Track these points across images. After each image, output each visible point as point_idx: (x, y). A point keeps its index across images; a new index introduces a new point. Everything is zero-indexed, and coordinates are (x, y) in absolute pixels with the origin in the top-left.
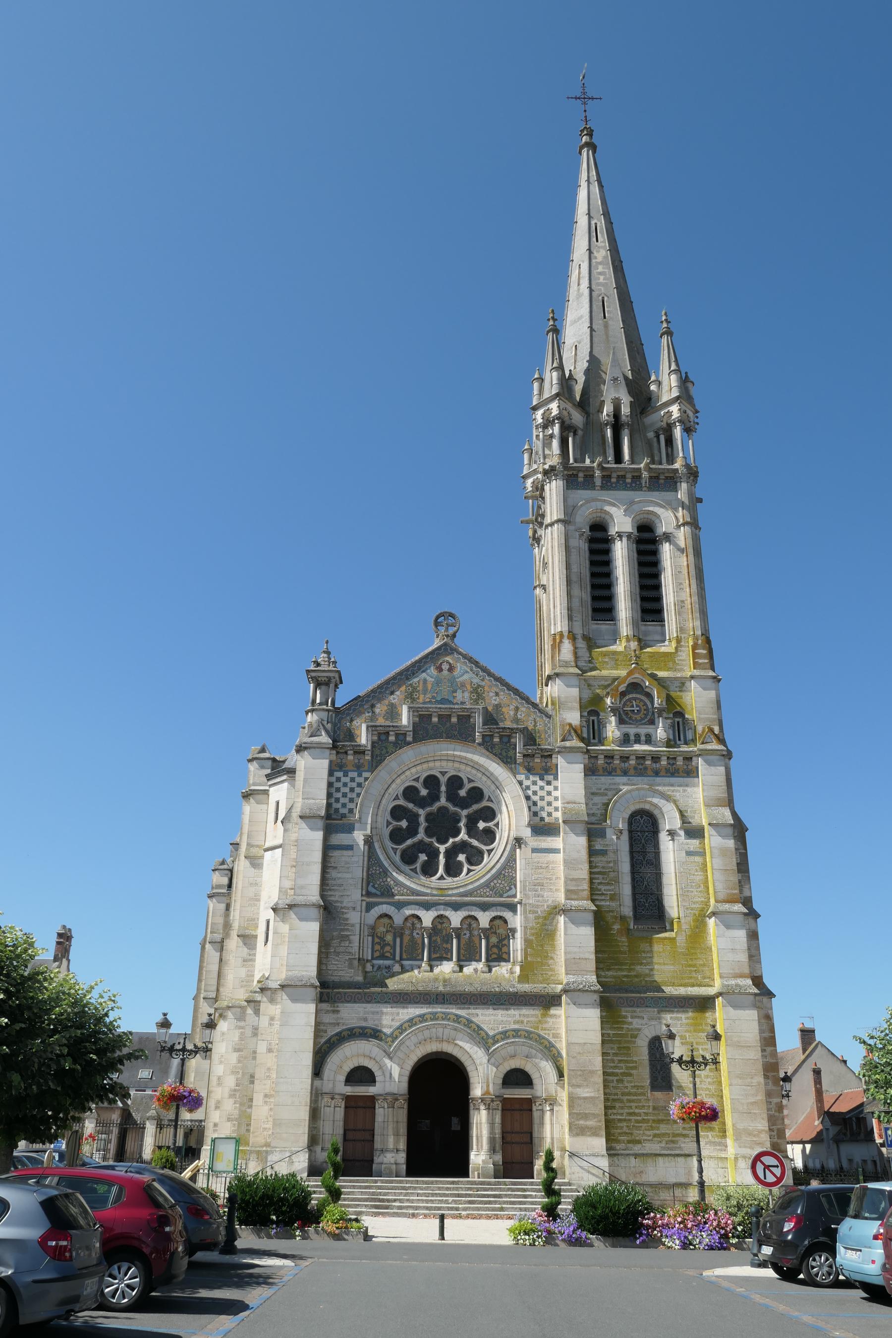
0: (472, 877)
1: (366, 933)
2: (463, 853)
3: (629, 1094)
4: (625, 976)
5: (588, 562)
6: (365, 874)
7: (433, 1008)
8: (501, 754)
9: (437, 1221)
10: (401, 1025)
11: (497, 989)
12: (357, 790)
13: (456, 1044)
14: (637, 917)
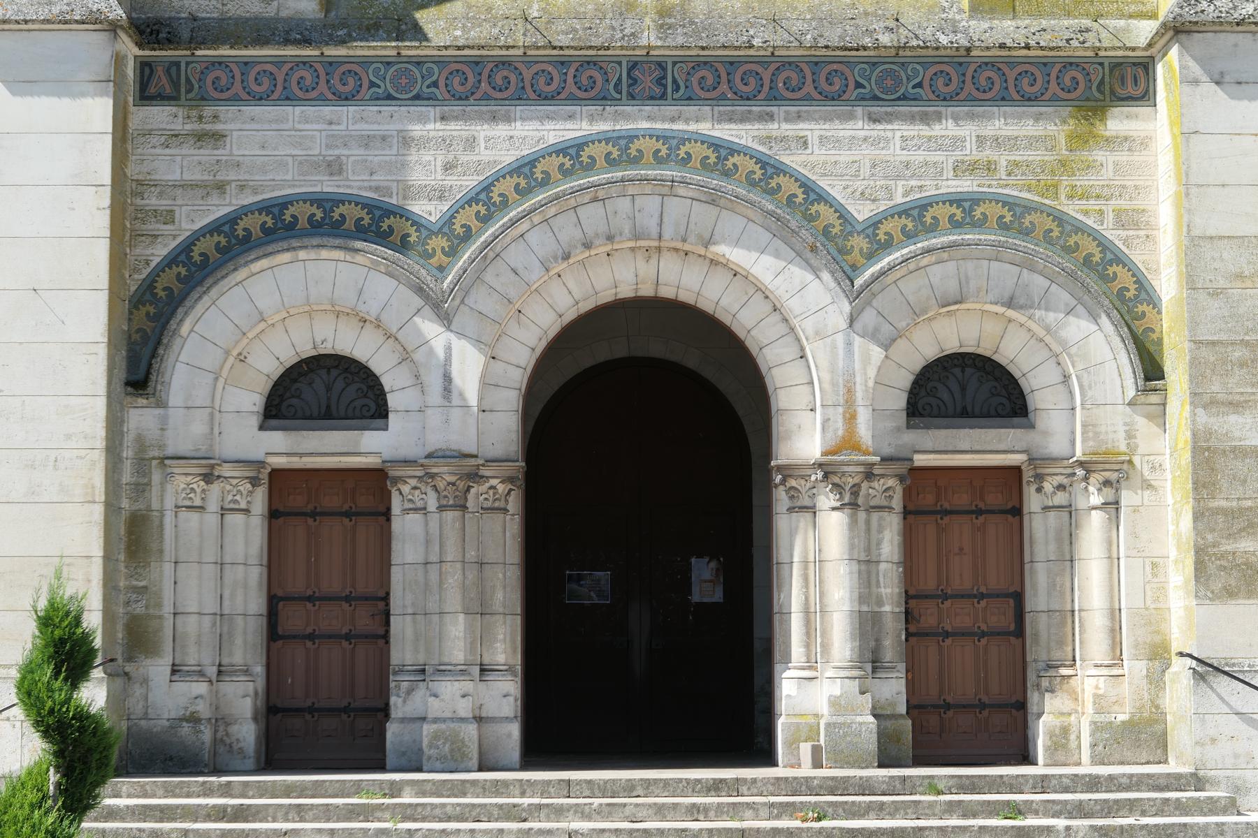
7: (617, 117)
10: (487, 189)
11: (885, 39)
13: (714, 262)
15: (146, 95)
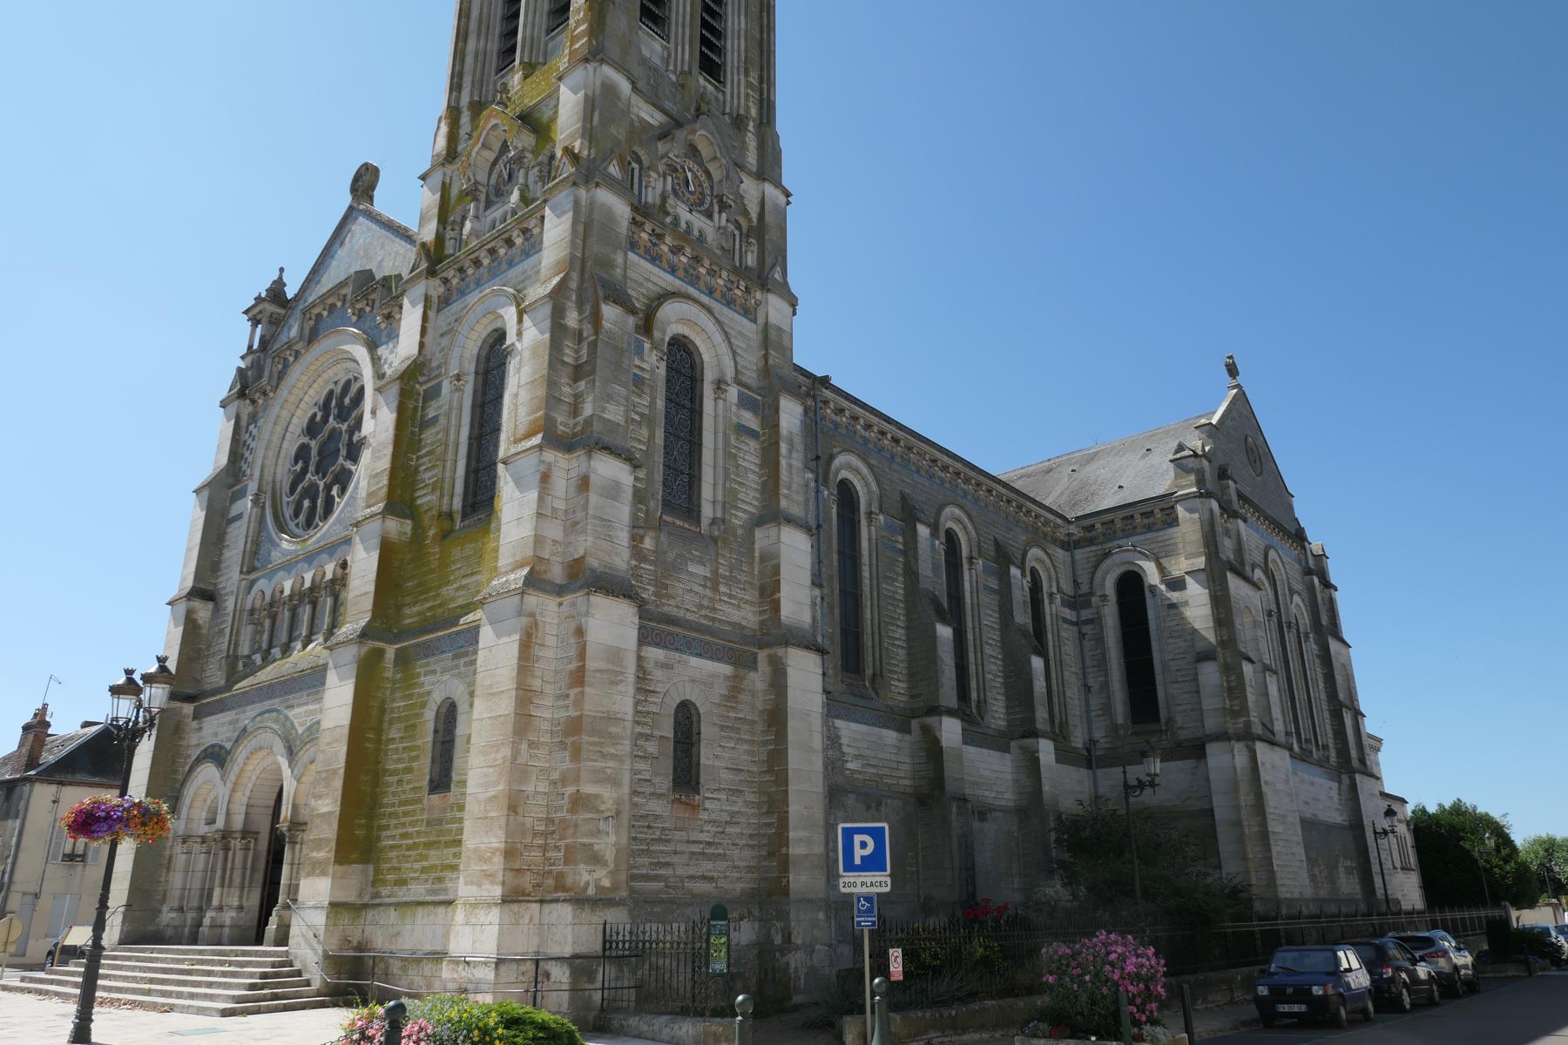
4: (430, 609)
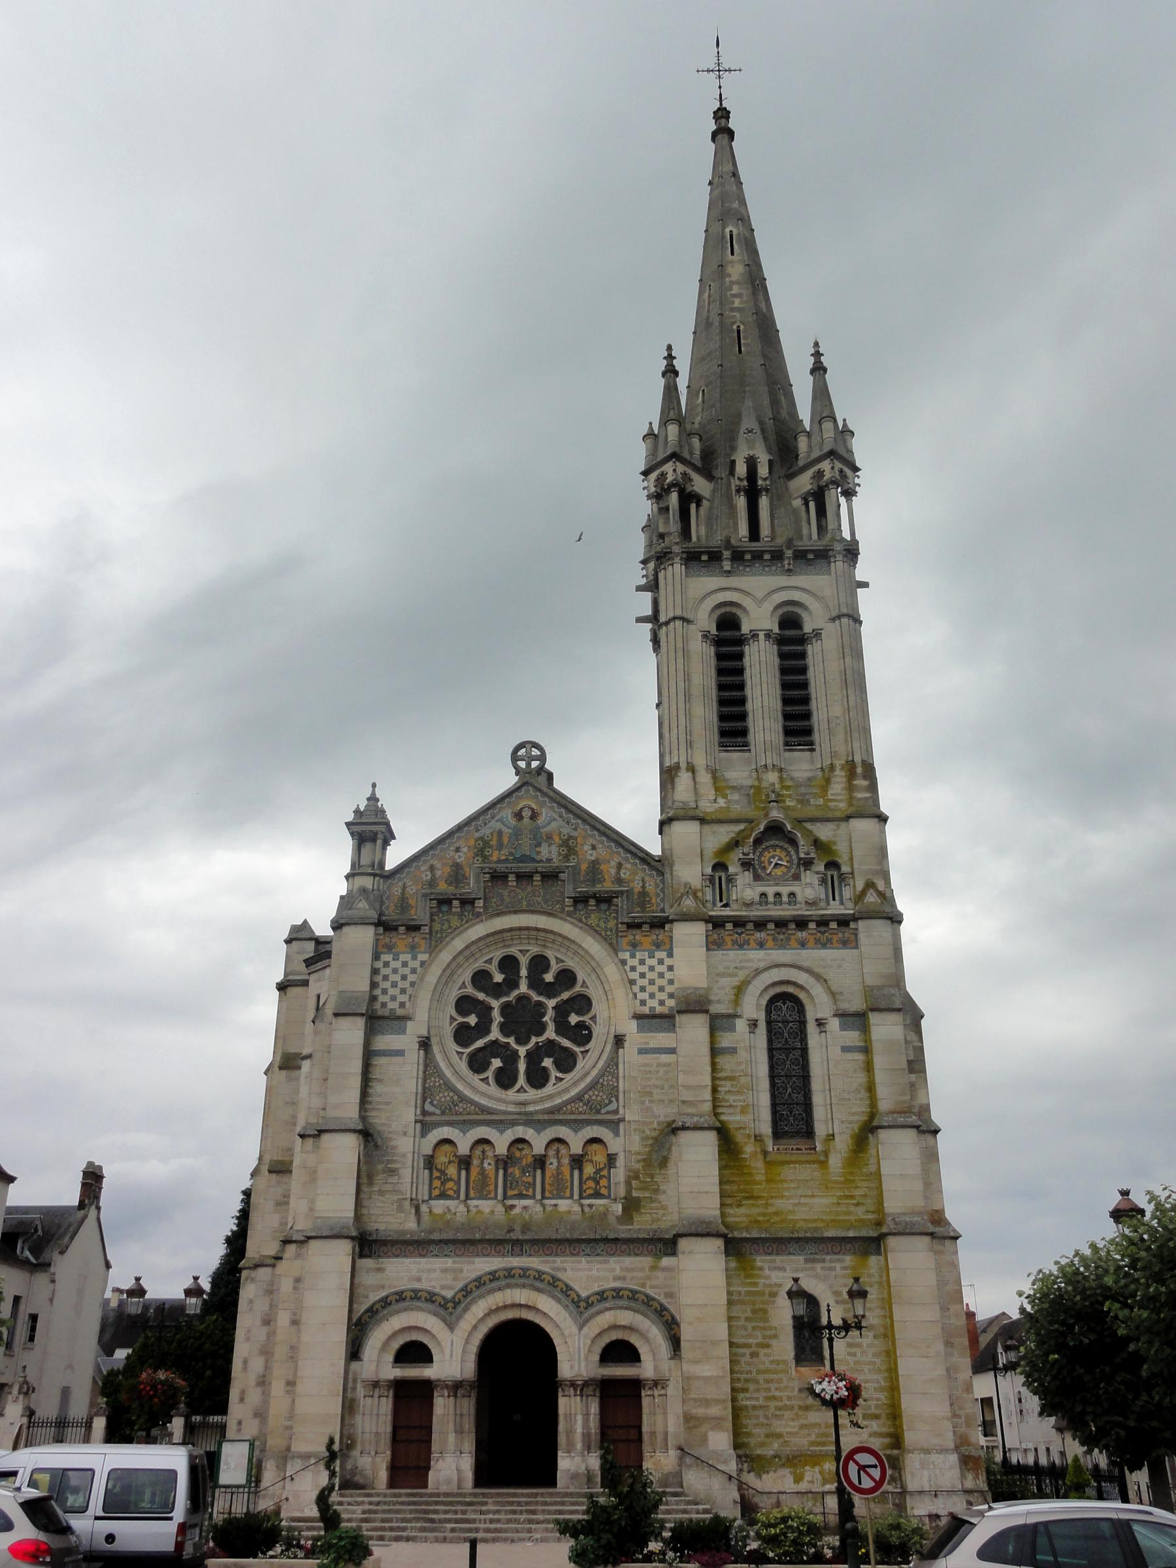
0: (561, 1089)
1: (422, 1165)
2: (549, 1057)
3: (766, 1371)
4: (764, 1215)
5: (713, 670)
6: (420, 1087)
8: (598, 925)
9: (468, 1545)
12: (412, 978)
14: (777, 1134)
15: (361, 1256)
